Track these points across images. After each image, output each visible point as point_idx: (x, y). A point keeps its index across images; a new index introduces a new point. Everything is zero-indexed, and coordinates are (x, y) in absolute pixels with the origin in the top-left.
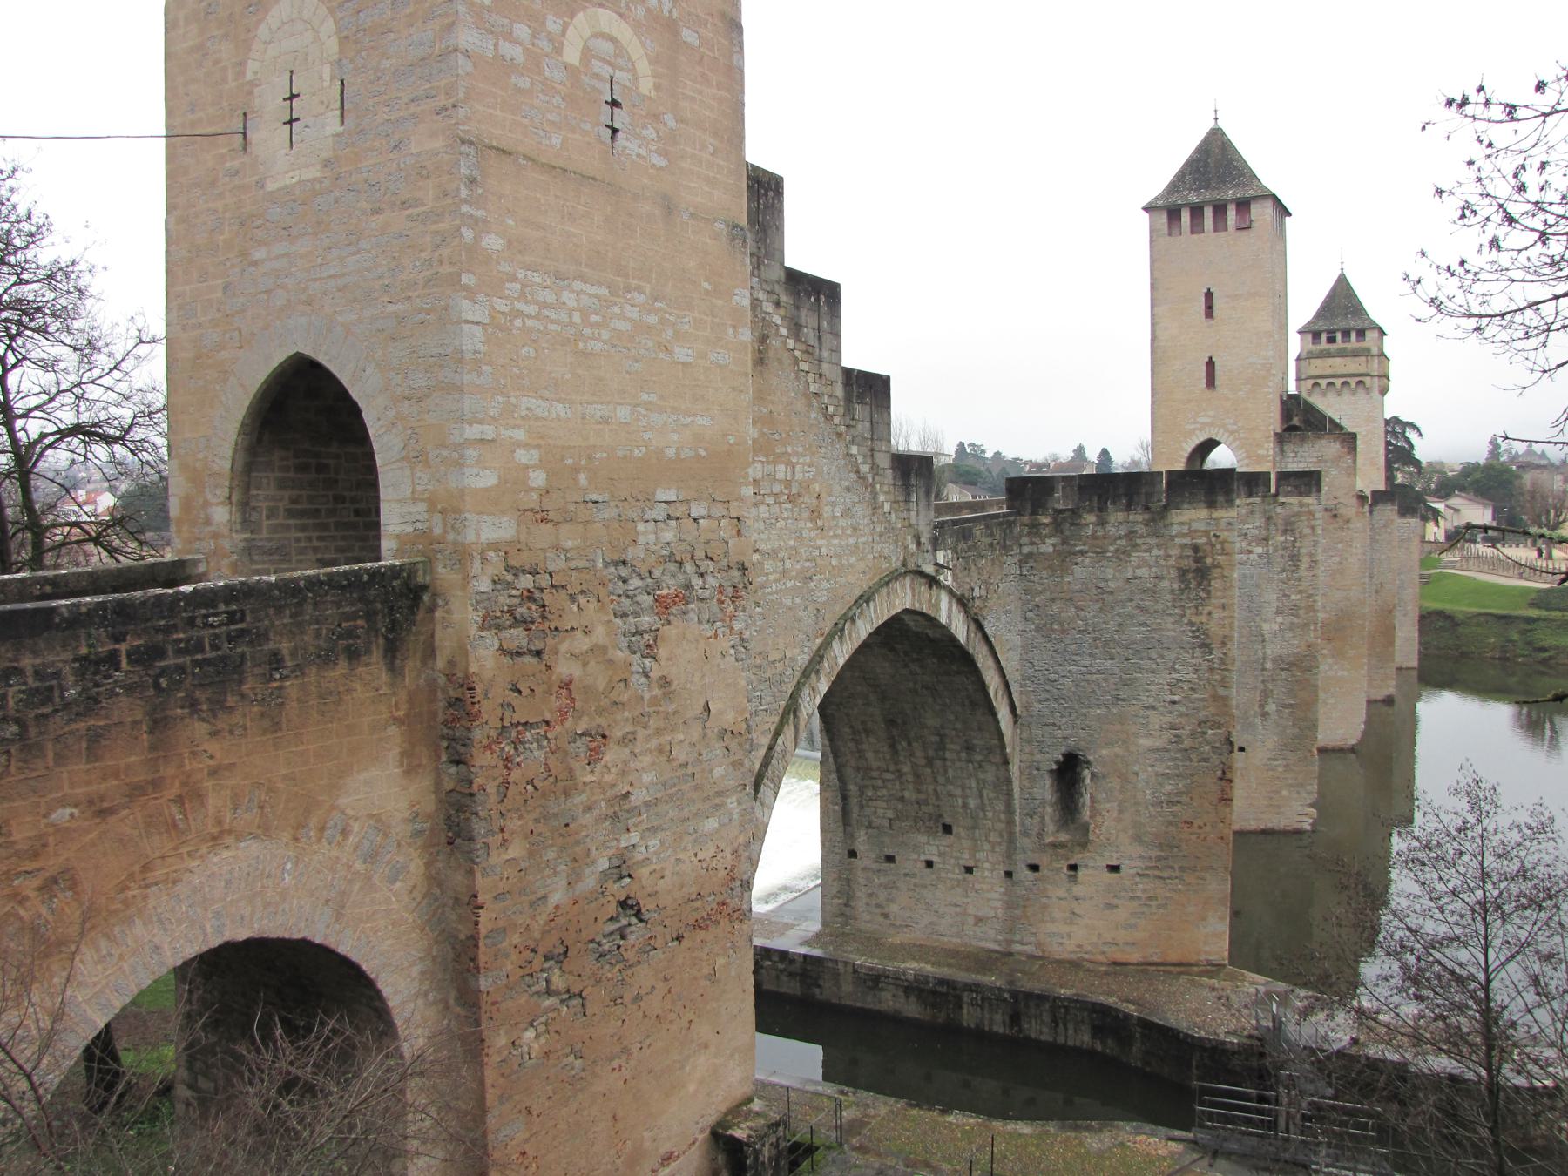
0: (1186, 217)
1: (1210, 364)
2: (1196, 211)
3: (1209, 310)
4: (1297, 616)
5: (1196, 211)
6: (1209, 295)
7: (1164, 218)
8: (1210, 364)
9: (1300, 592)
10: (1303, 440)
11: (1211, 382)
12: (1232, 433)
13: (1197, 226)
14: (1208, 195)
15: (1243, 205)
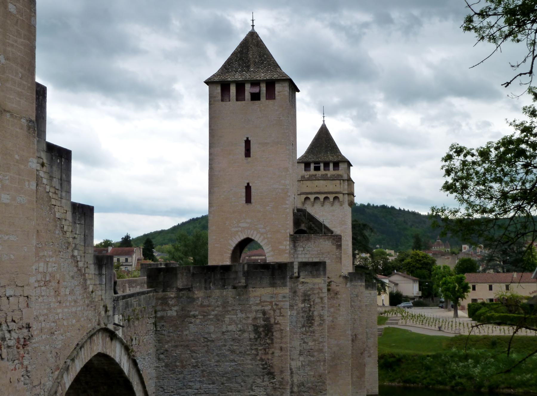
0: (233, 89)
1: (248, 188)
2: (240, 86)
3: (248, 153)
4: (313, 356)
5: (240, 86)
6: (248, 142)
7: (218, 89)
8: (248, 188)
9: (314, 340)
10: (308, 239)
11: (248, 200)
12: (262, 234)
13: (240, 96)
14: (247, 76)
15: (271, 84)
